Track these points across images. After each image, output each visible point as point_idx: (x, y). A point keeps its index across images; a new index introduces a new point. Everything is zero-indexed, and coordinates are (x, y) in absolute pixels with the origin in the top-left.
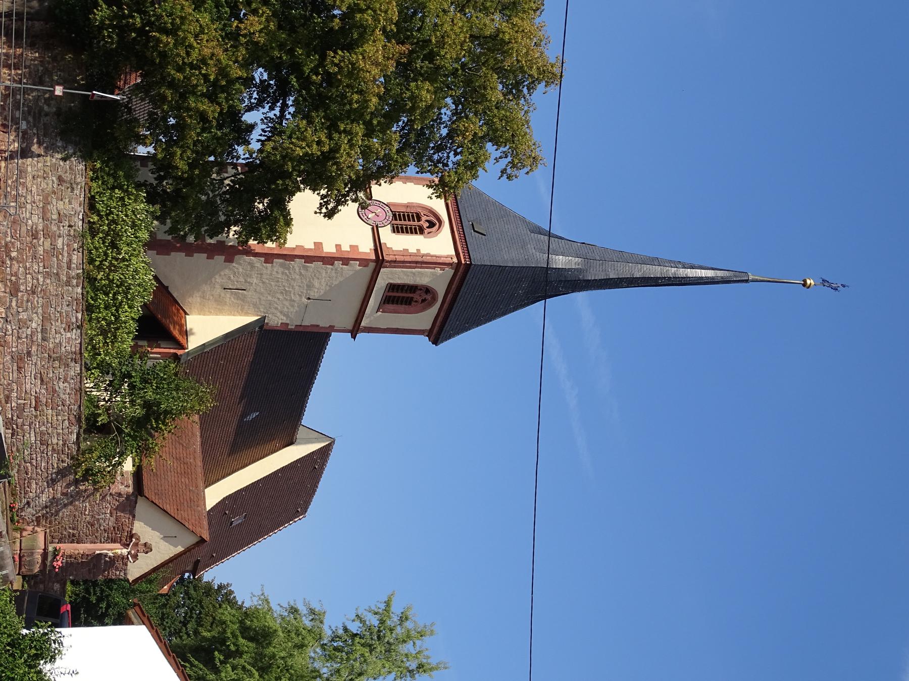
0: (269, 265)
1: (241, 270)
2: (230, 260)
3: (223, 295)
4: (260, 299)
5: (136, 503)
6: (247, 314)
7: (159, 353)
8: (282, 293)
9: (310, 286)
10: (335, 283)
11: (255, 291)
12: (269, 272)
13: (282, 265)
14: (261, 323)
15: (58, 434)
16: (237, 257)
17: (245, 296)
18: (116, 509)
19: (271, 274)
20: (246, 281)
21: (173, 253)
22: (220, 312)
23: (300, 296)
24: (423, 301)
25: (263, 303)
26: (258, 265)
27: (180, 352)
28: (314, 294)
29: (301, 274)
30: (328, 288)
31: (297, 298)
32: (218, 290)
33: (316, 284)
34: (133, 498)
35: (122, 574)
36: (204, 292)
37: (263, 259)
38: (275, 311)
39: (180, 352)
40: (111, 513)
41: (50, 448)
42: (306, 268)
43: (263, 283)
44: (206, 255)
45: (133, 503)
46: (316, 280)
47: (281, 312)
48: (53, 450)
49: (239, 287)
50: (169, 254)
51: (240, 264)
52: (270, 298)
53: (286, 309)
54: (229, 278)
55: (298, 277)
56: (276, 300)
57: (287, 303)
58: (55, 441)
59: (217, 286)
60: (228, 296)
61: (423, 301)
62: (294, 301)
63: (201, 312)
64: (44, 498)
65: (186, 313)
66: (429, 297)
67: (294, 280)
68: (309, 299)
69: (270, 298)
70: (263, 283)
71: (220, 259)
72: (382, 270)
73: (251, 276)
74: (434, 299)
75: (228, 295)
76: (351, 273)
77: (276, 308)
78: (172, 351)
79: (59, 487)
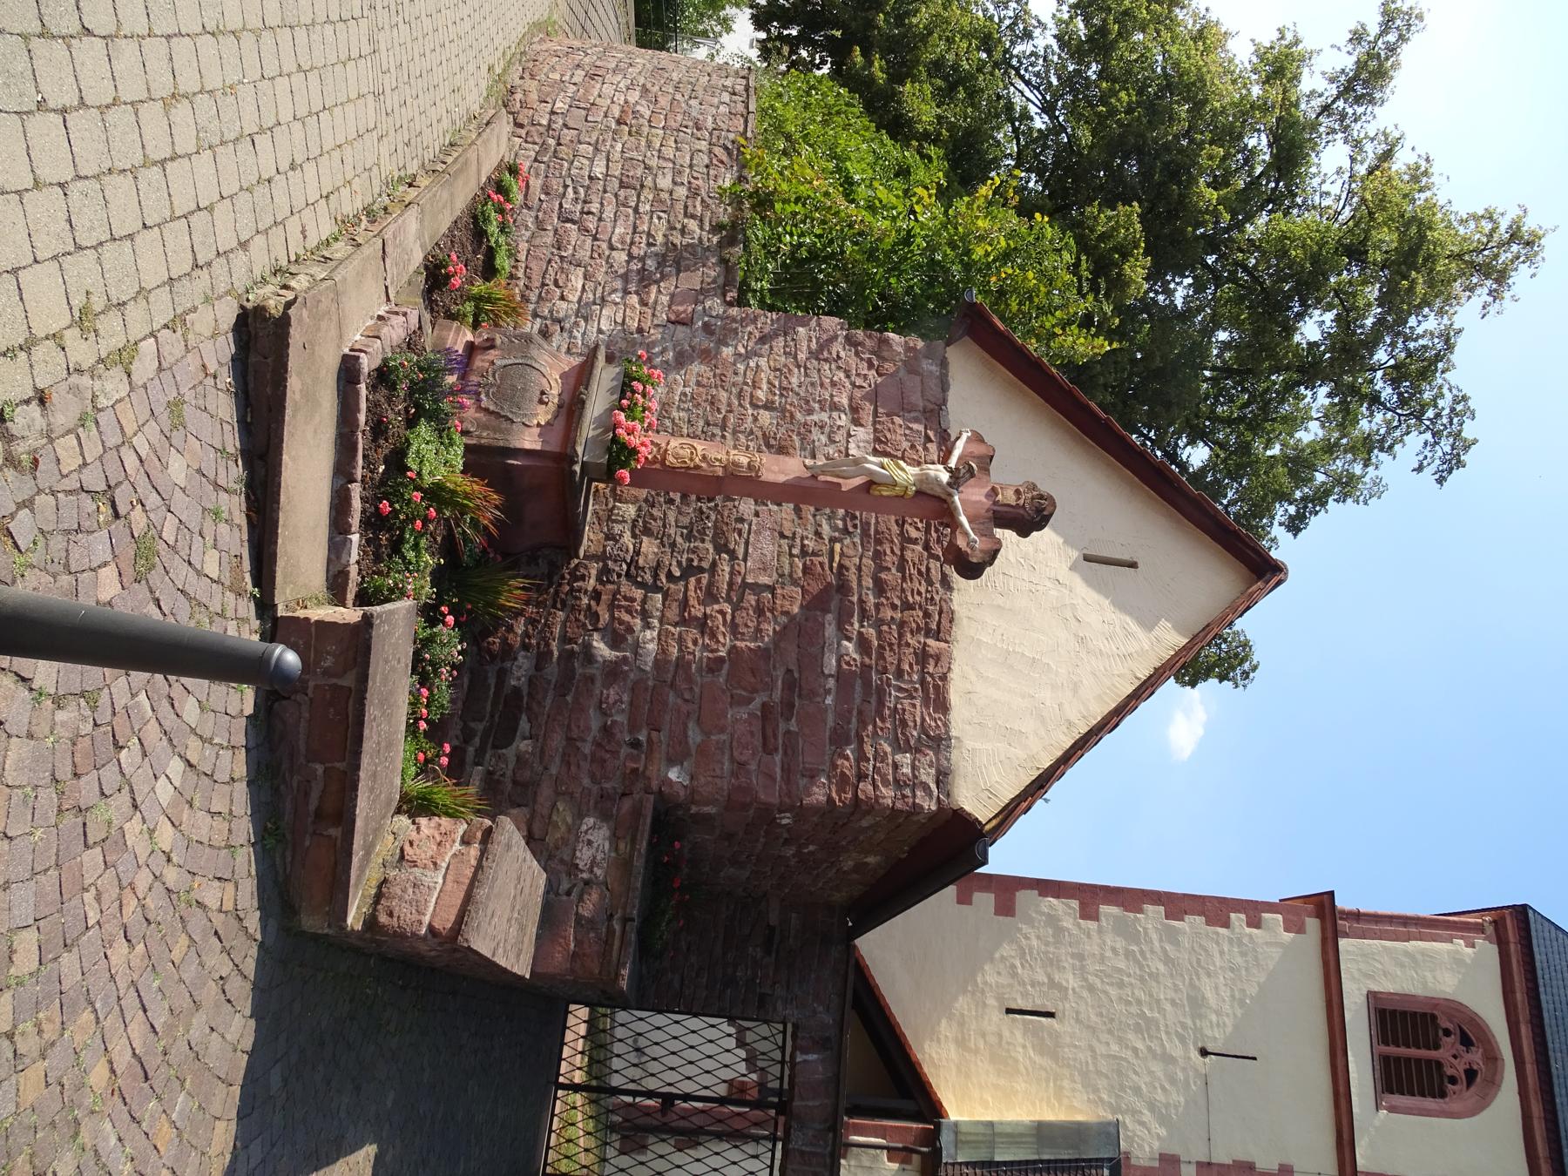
0: (1092, 925)
1: (1035, 942)
3: (1006, 1034)
5: (944, 387)
8: (1138, 1029)
9: (1197, 1004)
10: (1253, 990)
13: (1121, 929)
15: (677, 172)
17: (1055, 1036)
18: (875, 396)
20: (1053, 984)
23: (1182, 1040)
24: (1471, 1075)
25: (1104, 1066)
26: (1068, 923)
30: (1239, 1012)
31: (1176, 1050)
32: (996, 1017)
34: (929, 366)
35: (927, 776)
37: (1075, 904)
38: (1139, 1104)
40: (855, 409)
41: (647, 195)
42: (1172, 937)
43: (1091, 989)
45: (933, 384)
46: (1204, 979)
47: (1152, 1107)
48: (657, 200)
51: (1030, 922)
53: (1160, 1096)
54: (1014, 975)
55: (1162, 967)
56: (1128, 1054)
57: (1157, 1068)
58: (665, 182)
60: (1019, 1035)
61: (1471, 1075)
64: (606, 320)
66: (1476, 1057)
67: (1155, 976)
68: (1204, 1053)
70: (1091, 989)
72: (1343, 943)
73: (1061, 969)
74: (1493, 1058)
76: (1275, 953)
77: (1137, 1090)
79: (660, 295)
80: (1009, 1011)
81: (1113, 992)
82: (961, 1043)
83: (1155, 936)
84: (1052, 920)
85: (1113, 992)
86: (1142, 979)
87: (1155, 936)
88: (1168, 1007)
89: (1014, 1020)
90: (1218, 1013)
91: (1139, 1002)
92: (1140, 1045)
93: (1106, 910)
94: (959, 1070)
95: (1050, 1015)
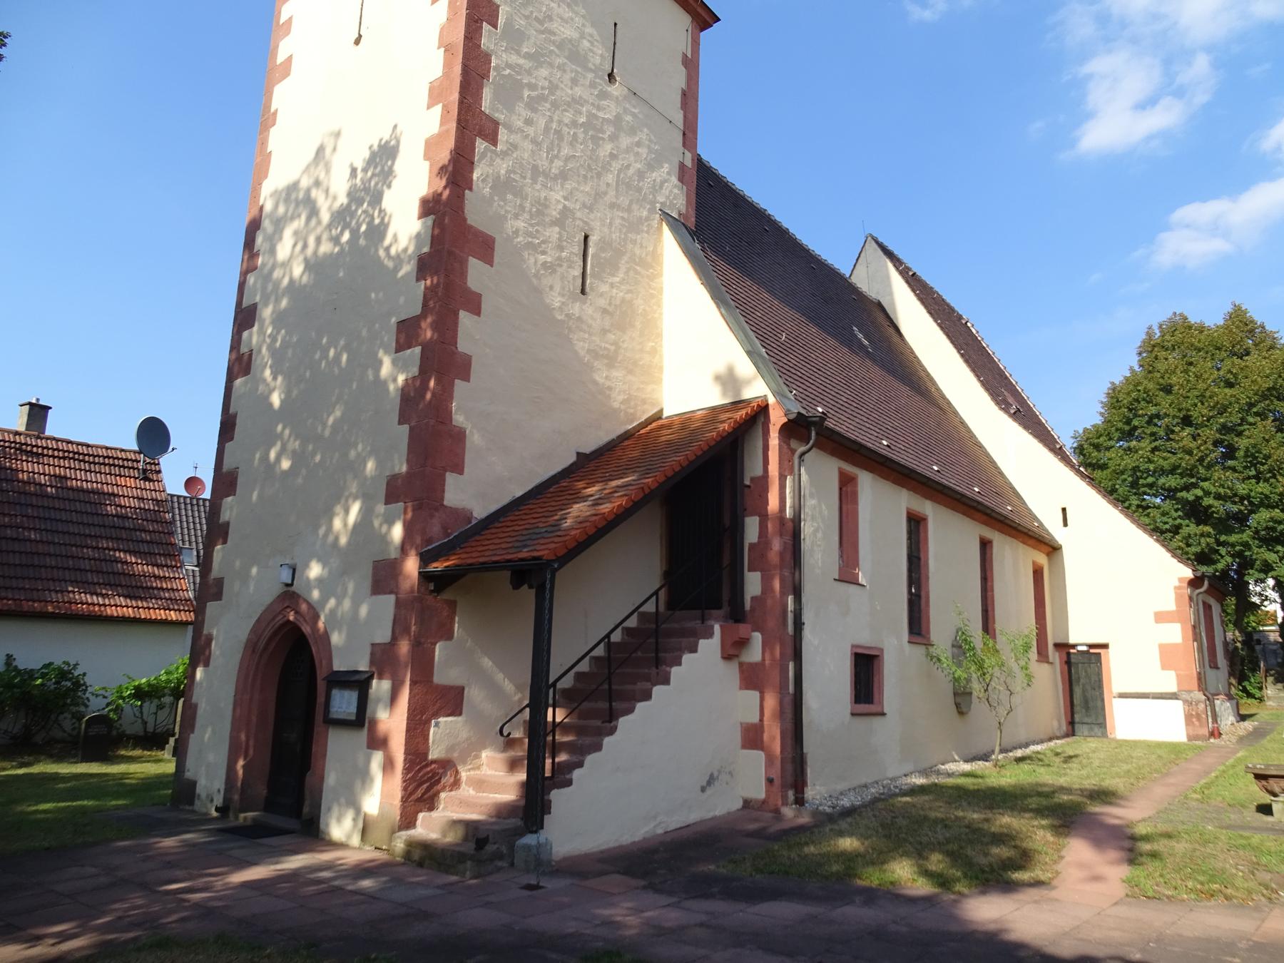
0: (503, 134)
1: (521, 224)
2: (485, 247)
3: (602, 302)
4: (613, 206)
6: (656, 256)
7: (782, 479)
9: (576, 57)
11: (591, 209)
12: (527, 145)
14: (676, 224)
16: (475, 213)
17: (605, 244)
19: (534, 141)
20: (559, 222)
21: (459, 419)
22: (651, 327)
23: (604, 95)
26: (502, 167)
27: (777, 418)
28: (599, 56)
29: (537, 58)
31: (610, 111)
32: (587, 310)
33: (568, 32)
36: (595, 354)
37: (481, 145)
39: (777, 418)
44: (464, 317)
49: (577, 249)
50: (459, 436)
52: (610, 178)
55: (544, 72)
56: (616, 165)
57: (625, 141)
59: (576, 309)
60: (604, 288)
62: (618, 118)
63: (651, 373)
65: (658, 416)
68: (611, 76)
69: (610, 178)
71: (477, 274)
75: (605, 289)
77: (641, 175)
78: (774, 441)
80: (583, 292)
81: (566, 151)
82: (611, 360)
83: (514, 59)
84: (503, 186)
85: (566, 151)
86: (555, 105)
87: (514, 59)
88: (578, 91)
89: (592, 289)
90: (582, 36)
91: (574, 124)
92: (608, 147)
93: (487, 101)
94: (631, 372)
95: (586, 237)
